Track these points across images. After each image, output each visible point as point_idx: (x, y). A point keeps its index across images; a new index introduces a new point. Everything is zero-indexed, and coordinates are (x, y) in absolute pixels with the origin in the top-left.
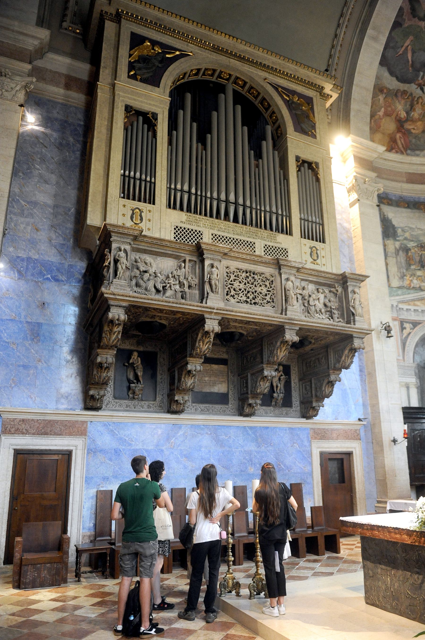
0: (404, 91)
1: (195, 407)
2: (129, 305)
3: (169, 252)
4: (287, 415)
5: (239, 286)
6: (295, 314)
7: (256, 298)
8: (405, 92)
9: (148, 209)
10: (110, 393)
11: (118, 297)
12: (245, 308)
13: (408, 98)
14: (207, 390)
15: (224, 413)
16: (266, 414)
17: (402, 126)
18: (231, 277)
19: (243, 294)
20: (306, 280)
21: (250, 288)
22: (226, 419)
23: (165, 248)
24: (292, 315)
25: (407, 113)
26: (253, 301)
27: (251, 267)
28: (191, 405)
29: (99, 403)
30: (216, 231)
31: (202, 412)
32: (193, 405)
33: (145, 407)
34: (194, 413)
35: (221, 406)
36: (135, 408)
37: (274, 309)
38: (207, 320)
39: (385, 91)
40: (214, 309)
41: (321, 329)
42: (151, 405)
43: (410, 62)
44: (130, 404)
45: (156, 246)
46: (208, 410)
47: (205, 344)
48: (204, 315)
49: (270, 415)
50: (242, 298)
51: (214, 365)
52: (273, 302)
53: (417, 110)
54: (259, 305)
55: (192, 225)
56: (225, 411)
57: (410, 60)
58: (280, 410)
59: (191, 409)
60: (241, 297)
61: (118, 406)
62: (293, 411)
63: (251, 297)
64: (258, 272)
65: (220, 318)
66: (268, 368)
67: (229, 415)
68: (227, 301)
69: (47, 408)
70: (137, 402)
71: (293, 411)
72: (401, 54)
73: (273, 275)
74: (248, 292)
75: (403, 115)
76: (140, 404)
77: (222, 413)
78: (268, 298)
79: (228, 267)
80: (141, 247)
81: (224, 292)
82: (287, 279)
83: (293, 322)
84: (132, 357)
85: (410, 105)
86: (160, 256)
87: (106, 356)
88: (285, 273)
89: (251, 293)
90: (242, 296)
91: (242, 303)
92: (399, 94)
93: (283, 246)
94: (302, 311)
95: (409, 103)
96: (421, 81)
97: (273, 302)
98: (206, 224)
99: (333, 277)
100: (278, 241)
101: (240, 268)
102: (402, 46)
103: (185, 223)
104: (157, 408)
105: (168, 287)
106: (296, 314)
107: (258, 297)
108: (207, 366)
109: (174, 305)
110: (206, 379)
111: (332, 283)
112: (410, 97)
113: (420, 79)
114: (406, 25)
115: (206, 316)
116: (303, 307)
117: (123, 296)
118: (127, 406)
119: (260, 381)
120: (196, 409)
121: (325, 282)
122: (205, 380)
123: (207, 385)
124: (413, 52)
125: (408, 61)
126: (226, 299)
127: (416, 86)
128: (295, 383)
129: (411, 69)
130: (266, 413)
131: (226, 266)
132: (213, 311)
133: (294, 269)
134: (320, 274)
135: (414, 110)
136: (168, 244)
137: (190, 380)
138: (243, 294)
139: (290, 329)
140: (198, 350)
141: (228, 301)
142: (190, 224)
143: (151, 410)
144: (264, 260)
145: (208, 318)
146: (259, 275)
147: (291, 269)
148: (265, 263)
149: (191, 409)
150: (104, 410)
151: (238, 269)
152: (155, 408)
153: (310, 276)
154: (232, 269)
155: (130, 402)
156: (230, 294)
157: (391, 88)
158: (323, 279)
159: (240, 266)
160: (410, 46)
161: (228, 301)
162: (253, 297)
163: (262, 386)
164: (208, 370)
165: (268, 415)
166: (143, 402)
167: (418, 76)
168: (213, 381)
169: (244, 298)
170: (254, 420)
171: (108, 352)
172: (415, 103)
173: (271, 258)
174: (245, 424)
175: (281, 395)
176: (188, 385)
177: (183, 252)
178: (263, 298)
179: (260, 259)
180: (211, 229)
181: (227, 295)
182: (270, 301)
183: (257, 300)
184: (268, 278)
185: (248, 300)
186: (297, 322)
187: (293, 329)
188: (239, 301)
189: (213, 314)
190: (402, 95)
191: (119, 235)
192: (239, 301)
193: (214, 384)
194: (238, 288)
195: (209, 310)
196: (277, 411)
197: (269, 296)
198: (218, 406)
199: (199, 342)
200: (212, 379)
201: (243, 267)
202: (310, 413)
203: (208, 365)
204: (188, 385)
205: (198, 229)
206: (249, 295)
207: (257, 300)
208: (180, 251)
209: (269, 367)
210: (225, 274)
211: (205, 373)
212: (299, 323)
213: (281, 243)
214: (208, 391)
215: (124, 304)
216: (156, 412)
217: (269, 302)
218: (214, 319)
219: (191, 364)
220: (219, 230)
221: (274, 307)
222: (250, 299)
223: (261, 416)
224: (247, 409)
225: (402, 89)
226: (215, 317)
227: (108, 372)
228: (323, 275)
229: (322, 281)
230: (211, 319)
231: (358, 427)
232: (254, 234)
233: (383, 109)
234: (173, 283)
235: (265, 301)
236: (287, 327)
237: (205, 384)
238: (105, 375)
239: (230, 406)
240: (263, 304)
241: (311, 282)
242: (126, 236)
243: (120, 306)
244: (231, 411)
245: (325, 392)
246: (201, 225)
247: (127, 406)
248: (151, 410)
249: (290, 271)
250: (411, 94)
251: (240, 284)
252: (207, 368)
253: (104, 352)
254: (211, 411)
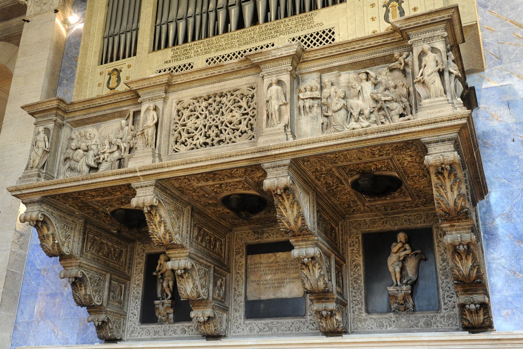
1: (249, 326)
3: (109, 112)
4: (428, 327)
5: (196, 123)
6: (274, 138)
7: (221, 133)
9: (127, 64)
10: (137, 316)
11: (24, 192)
12: (202, 153)
14: (268, 295)
15: (299, 332)
16: (381, 328)
18: (184, 114)
19: (201, 135)
20: (330, 70)
21: (214, 120)
22: (292, 342)
23: (103, 108)
24: (266, 141)
26: (217, 139)
27: (215, 87)
28: (242, 323)
29: (109, 332)
30: (213, 52)
31: (261, 333)
32: (247, 322)
33: (178, 331)
34: (248, 336)
35: (293, 320)
36: (165, 335)
37: (253, 140)
38: (137, 190)
40: (135, 172)
41: (335, 149)
42: (186, 329)
44: (159, 329)
45: (92, 110)
46: (271, 329)
47: (157, 226)
49: (389, 329)
50: (198, 141)
51: (280, 253)
52: (252, 129)
54: (226, 142)
55: (180, 60)
56: (299, 328)
58: (412, 317)
59: (243, 329)
60: (198, 139)
61: (144, 334)
62: (441, 317)
63: (213, 135)
64: (226, 90)
65: (153, 182)
66: (301, 243)
68: (174, 153)
69: (68, 343)
70: (168, 326)
71: (441, 317)
73: (254, 86)
74: (210, 127)
76: (172, 328)
77: (294, 332)
78: (243, 127)
79: (180, 102)
80: (77, 119)
81: (169, 141)
83: (269, 153)
84: (159, 262)
86: (104, 121)
87: (71, 268)
88: (269, 74)
89: (213, 128)
90: (199, 137)
91: (197, 148)
93: (326, 26)
94: (319, 127)
97: (252, 129)
98: (199, 50)
99: (381, 41)
100: (315, 24)
101: (198, 96)
103: (170, 61)
104: (194, 331)
105: (101, 159)
106: (277, 137)
107: (226, 130)
108: (270, 257)
109: (86, 182)
110: (269, 277)
111: (387, 53)
115: (134, 184)
116: (322, 120)
117: (27, 189)
118: (156, 333)
120: (251, 330)
121: (368, 57)
122: (266, 280)
123: (269, 288)
126: (174, 150)
128: (444, 260)
130: (381, 325)
131: (177, 100)
132: (136, 174)
133: (285, 61)
134: (350, 48)
136: (102, 102)
137: (186, 283)
138: (201, 135)
139: (273, 167)
140: (155, 236)
141: (176, 152)
142: (177, 60)
143: (185, 335)
144: (229, 69)
145: (137, 188)
146: (229, 94)
147: (280, 62)
148: (233, 72)
149: (243, 329)
150: (128, 340)
151: (196, 99)
152: (191, 333)
153: (335, 60)
154: (187, 101)
155: (160, 326)
156: (180, 141)
158: (364, 53)
159: (197, 93)
161: (176, 152)
162: (217, 134)
163: (309, 278)
164: (271, 263)
165: (384, 329)
166: (176, 325)
168: (279, 279)
169: (202, 140)
170: (347, 341)
171: (72, 263)
173: (236, 60)
175: (404, 288)
176: (188, 292)
177: (124, 104)
178: (233, 130)
179: (223, 70)
180: (206, 53)
181: (176, 142)
182: (246, 129)
183: (222, 137)
184: (245, 94)
185: (208, 141)
186: (277, 152)
187: (279, 166)
188: (193, 146)
189: (142, 180)
191: (43, 114)
192: (193, 146)
193: (280, 284)
194: (193, 127)
195: (131, 175)
196: (403, 320)
197: (245, 122)
198: (287, 321)
200: (279, 275)
201: (203, 92)
202: (469, 319)
203: (270, 254)
204: (188, 292)
205: (186, 62)
206: (210, 132)
207: (222, 137)
208: (121, 104)
209: (302, 241)
210: (175, 113)
211: (267, 269)
212: (281, 151)
213: (321, 24)
214: (272, 297)
215: (37, 198)
216: (191, 338)
217: (245, 132)
218: (146, 186)
219: (174, 259)
220: (217, 51)
221: (253, 137)
222: (211, 138)
223: (369, 333)
224: (323, 321)
226: (146, 183)
227: (86, 289)
228: (357, 47)
229: (361, 59)
230: (142, 187)
232: (273, 32)
234: (108, 151)
235: (237, 133)
236: (266, 165)
237: (266, 286)
238: (83, 292)
239: (309, 318)
240: (234, 139)
241: (341, 68)
242: (49, 113)
243: (34, 202)
244: (311, 327)
245: (459, 271)
246: (192, 55)
247: (156, 333)
248: (185, 335)
249: (278, 68)
251: (197, 121)
252: (270, 261)
253: (68, 263)
254: (275, 329)
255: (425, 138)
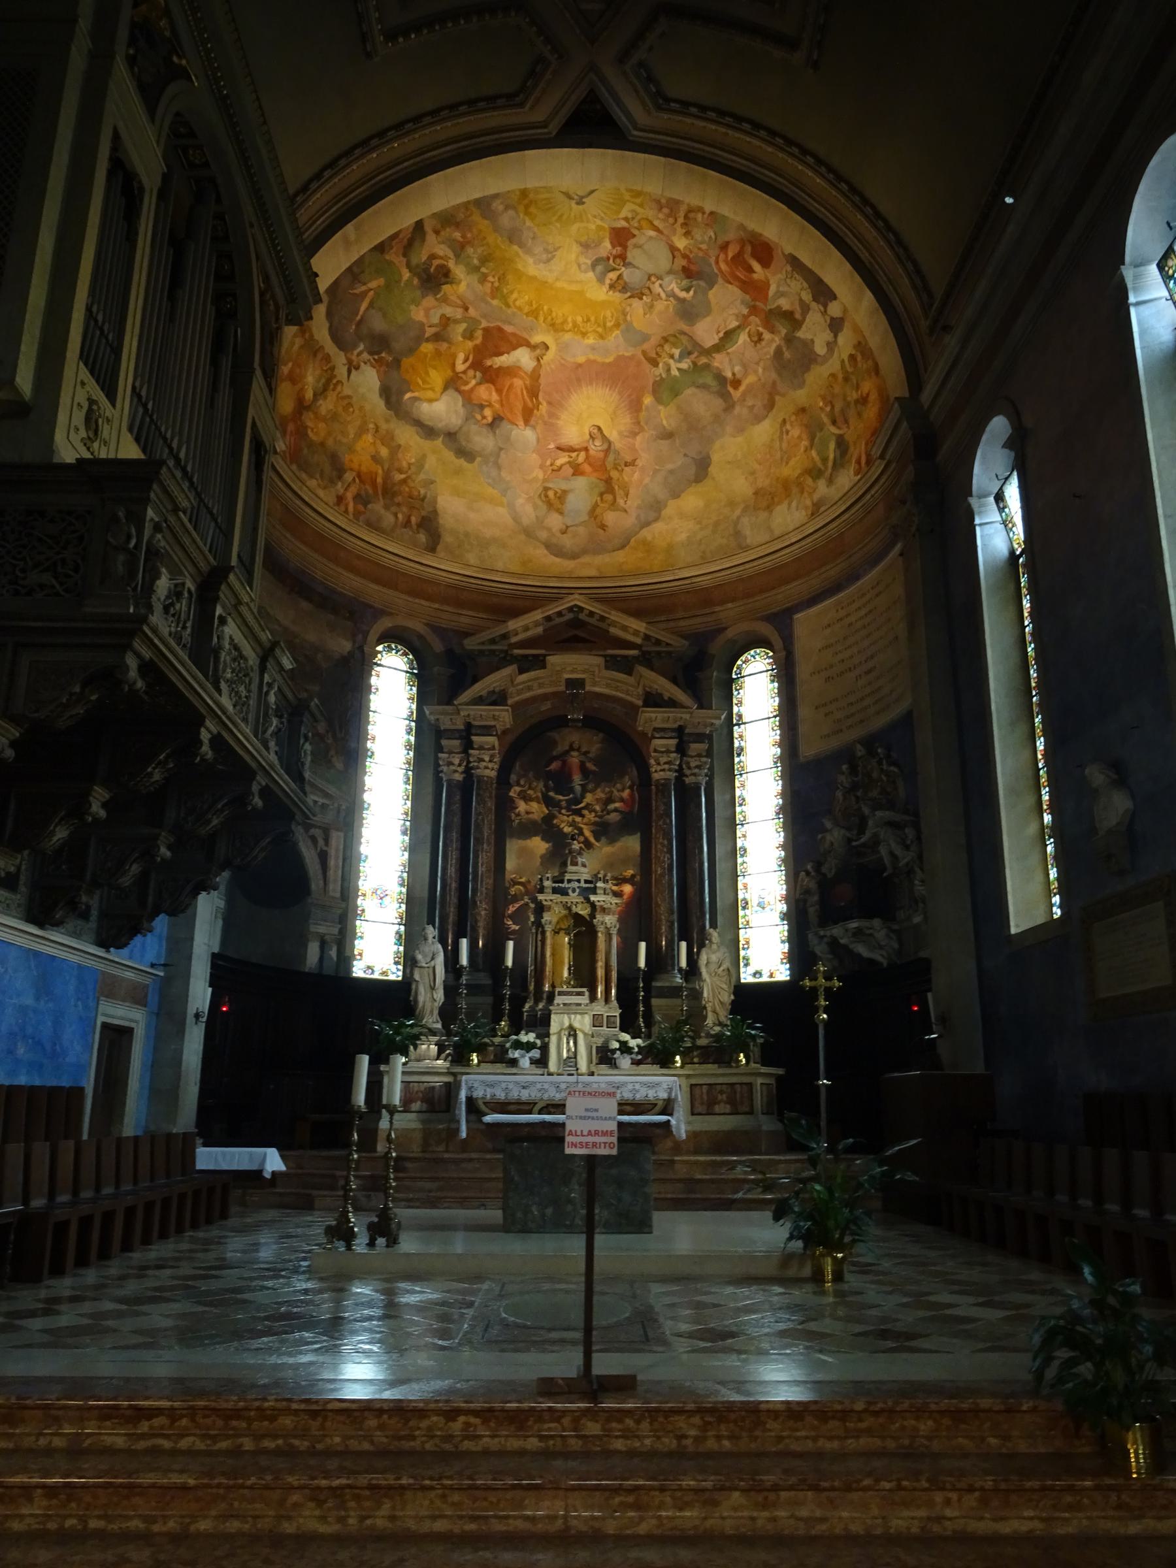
0: (328, 355)
2: (151, 659)
8: (327, 358)
13: (326, 371)
17: (301, 414)
25: (315, 395)
39: (307, 335)
43: (359, 318)
48: (205, 717)
53: (329, 398)
57: (361, 313)
67: (14, 917)
72: (355, 294)
75: (309, 395)
82: (270, 685)
85: (324, 385)
92: (320, 356)
95: (323, 380)
96: (354, 358)
102: (365, 284)
112: (329, 372)
113: (355, 352)
114: (387, 257)
119: (134, 861)
124: (371, 305)
125: (357, 315)
127: (345, 361)
129: (354, 327)
135: (325, 398)
157: (316, 337)
160: (372, 292)
167: (355, 346)
172: (332, 387)
174: (32, 944)
190: (322, 359)
199: (157, 765)
225: (327, 350)
231: (147, 981)
233: (290, 365)
250: (333, 369)
255: (297, 817)
